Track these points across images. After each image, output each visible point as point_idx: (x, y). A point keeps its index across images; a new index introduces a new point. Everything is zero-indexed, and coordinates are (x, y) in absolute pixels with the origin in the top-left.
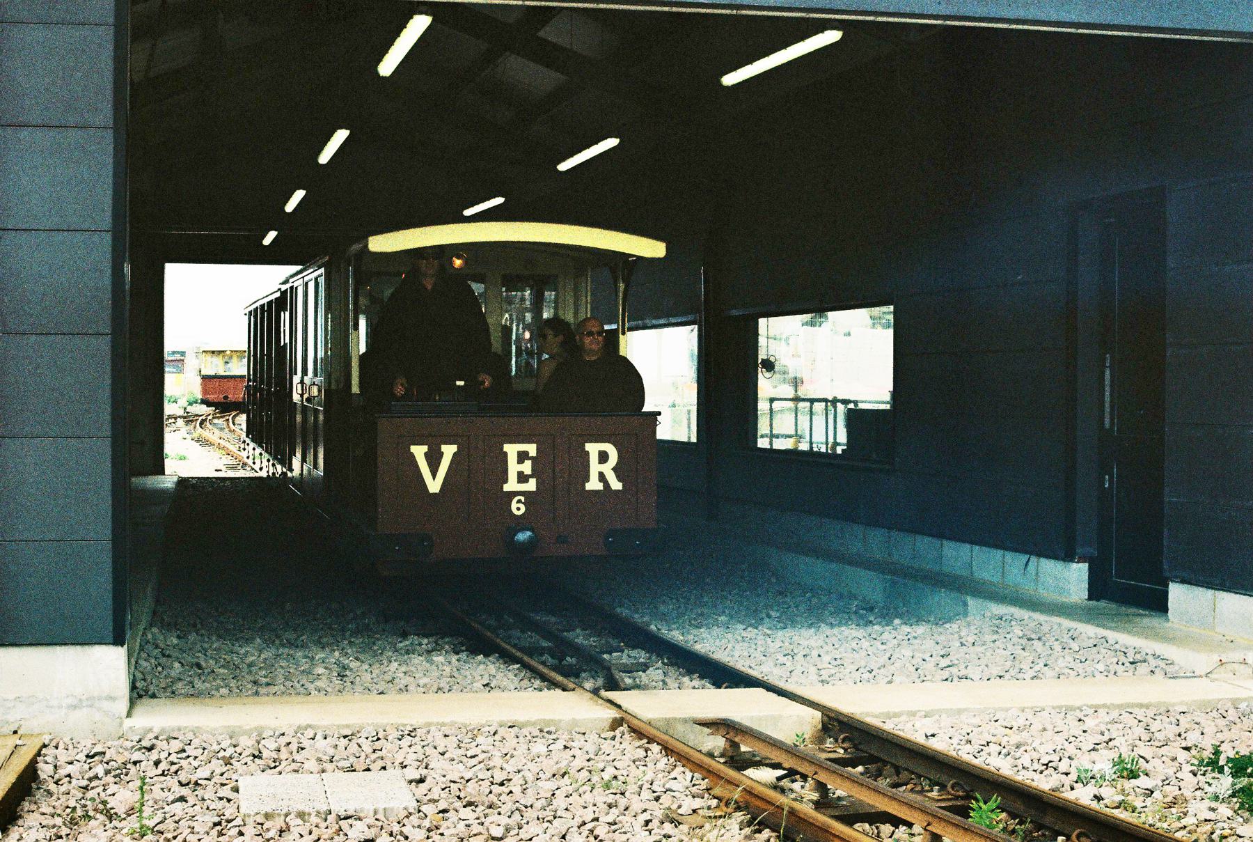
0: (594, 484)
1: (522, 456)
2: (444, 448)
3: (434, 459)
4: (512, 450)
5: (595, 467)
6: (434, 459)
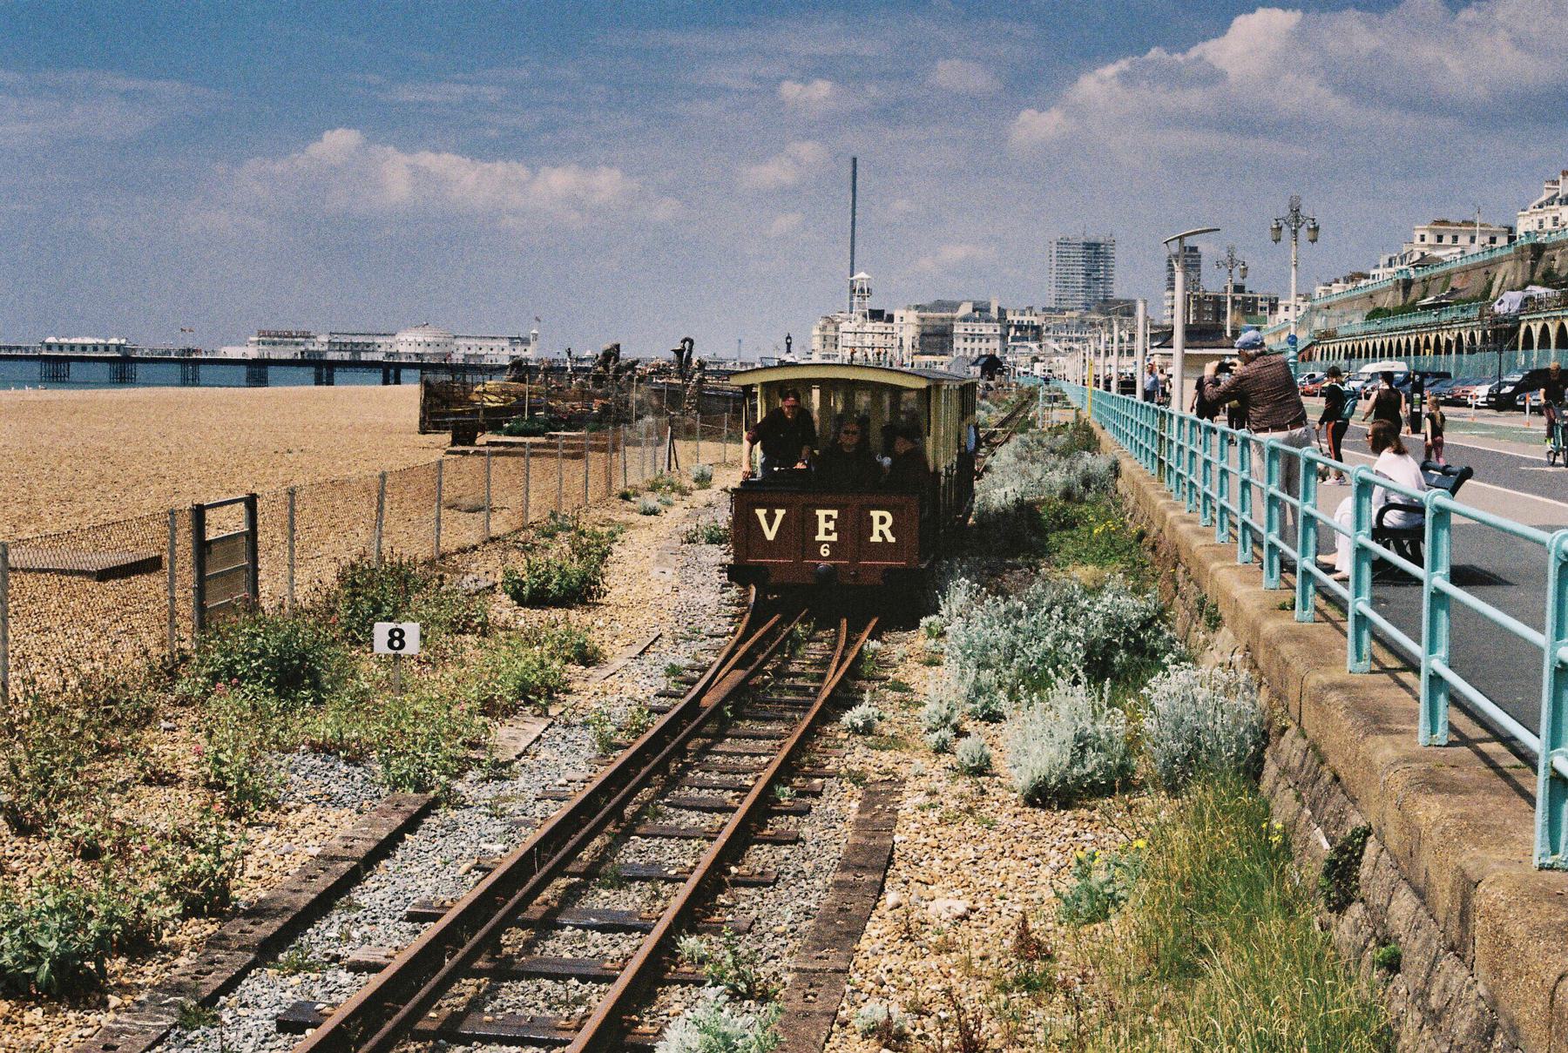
0: (876, 538)
1: (829, 518)
2: (777, 511)
3: (770, 518)
4: (821, 513)
5: (877, 527)
6: (770, 518)
